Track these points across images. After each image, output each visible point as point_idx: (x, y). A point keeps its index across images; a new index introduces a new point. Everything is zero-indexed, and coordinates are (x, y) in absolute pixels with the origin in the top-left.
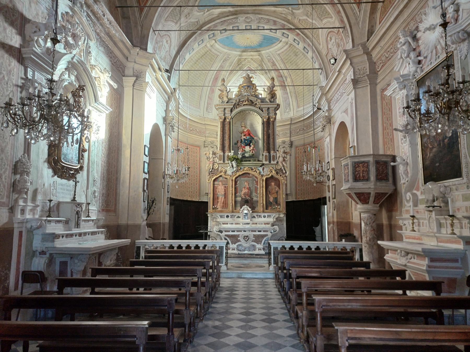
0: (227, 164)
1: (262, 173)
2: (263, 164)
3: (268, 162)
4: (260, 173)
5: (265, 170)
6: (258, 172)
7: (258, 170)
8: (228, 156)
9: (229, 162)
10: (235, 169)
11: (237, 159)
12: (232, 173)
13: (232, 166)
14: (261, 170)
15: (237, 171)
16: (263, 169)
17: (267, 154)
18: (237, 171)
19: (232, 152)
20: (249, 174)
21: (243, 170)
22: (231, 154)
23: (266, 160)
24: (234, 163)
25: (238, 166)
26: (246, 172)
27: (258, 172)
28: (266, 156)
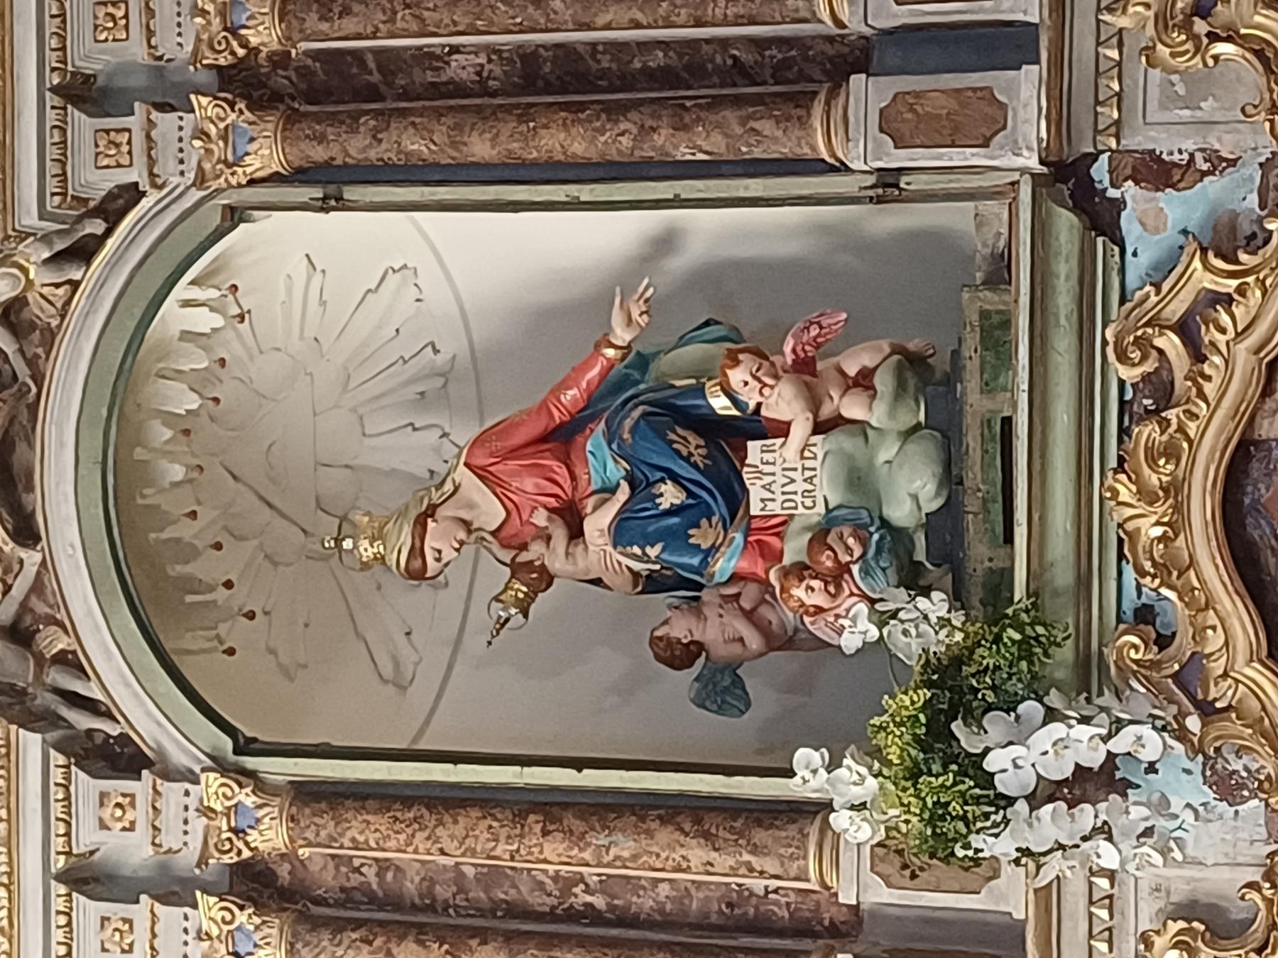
0: (1047, 898)
1: (1237, 192)
2: (1066, 177)
3: (1025, 88)
4: (1227, 240)
5: (1174, 146)
6: (1202, 277)
7: (1160, 273)
8: (893, 856)
9: (1001, 846)
10: (1151, 743)
11: (954, 693)
12: (1228, 788)
13: (1097, 782)
14: (1179, 209)
15: (1186, 687)
16: (1158, 173)
17: (867, 94)
18: (1186, 687)
19: (809, 774)
20: (1244, 455)
21: (1170, 568)
22: (855, 795)
23: (986, 122)
24: (1028, 751)
25: (1089, 679)
26: (1202, 506)
27: (1202, 277)
28: (894, 126)
